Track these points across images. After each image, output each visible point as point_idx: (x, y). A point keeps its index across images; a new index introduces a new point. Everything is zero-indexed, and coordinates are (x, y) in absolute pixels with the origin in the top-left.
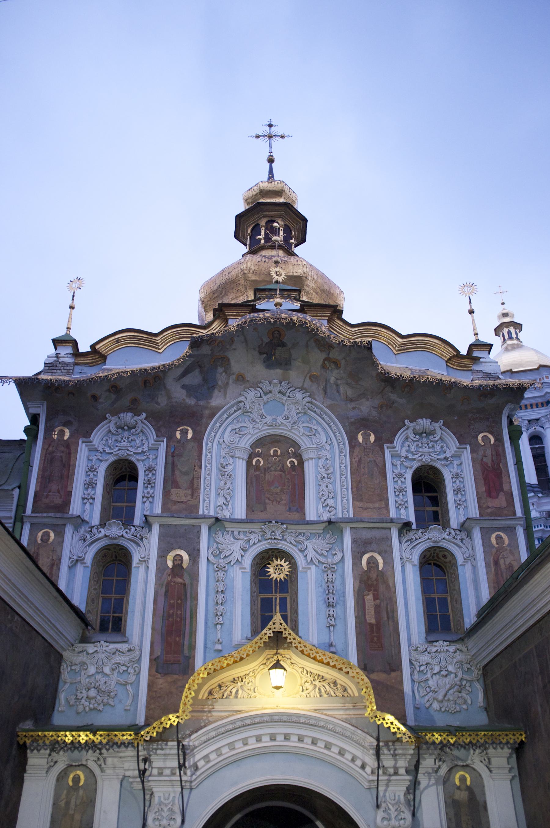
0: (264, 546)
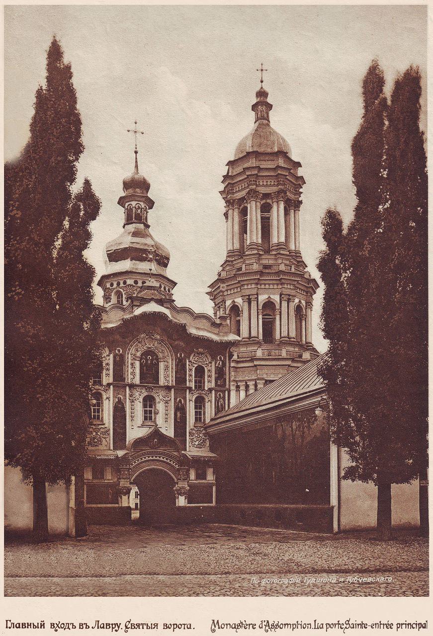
0: (146, 394)
